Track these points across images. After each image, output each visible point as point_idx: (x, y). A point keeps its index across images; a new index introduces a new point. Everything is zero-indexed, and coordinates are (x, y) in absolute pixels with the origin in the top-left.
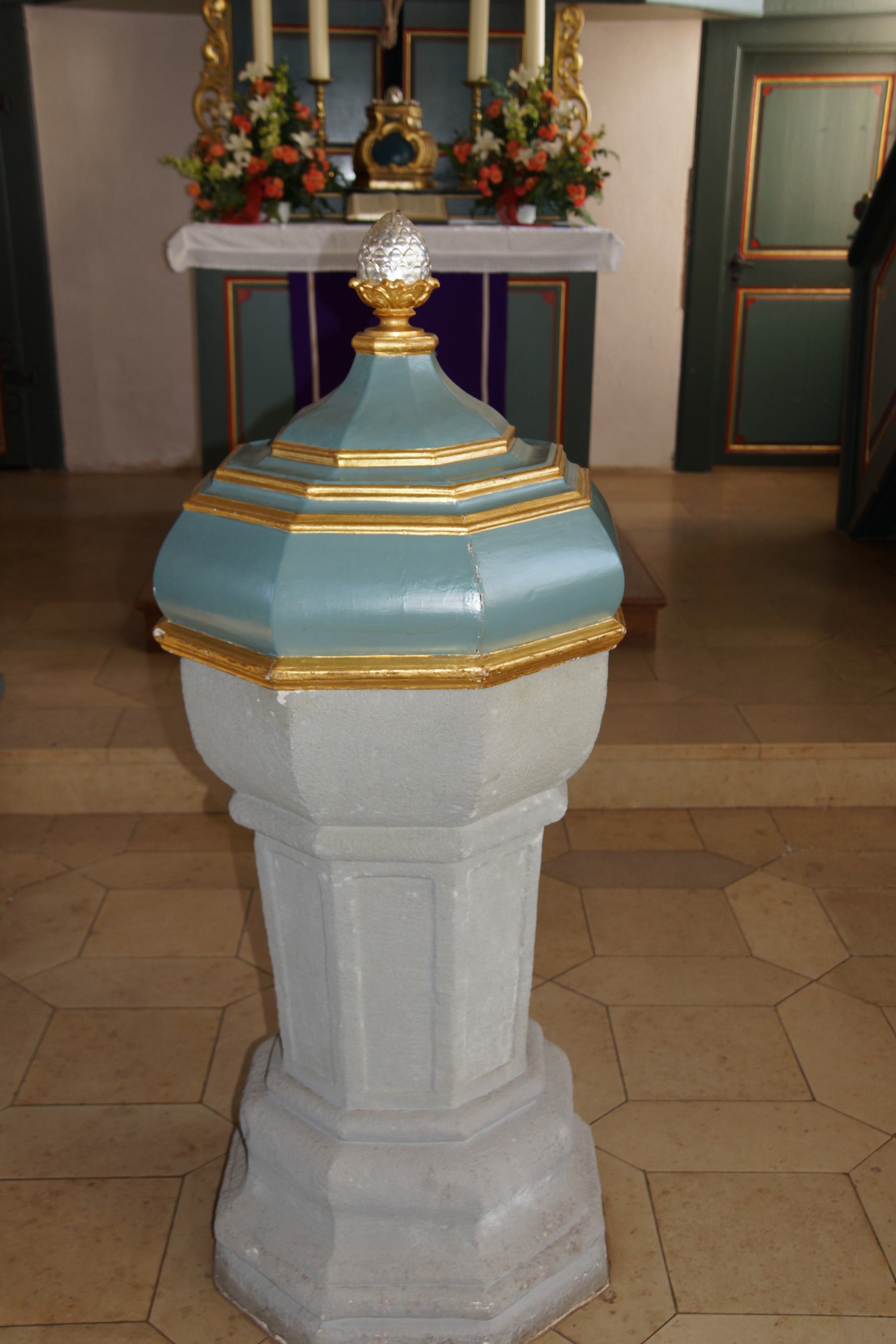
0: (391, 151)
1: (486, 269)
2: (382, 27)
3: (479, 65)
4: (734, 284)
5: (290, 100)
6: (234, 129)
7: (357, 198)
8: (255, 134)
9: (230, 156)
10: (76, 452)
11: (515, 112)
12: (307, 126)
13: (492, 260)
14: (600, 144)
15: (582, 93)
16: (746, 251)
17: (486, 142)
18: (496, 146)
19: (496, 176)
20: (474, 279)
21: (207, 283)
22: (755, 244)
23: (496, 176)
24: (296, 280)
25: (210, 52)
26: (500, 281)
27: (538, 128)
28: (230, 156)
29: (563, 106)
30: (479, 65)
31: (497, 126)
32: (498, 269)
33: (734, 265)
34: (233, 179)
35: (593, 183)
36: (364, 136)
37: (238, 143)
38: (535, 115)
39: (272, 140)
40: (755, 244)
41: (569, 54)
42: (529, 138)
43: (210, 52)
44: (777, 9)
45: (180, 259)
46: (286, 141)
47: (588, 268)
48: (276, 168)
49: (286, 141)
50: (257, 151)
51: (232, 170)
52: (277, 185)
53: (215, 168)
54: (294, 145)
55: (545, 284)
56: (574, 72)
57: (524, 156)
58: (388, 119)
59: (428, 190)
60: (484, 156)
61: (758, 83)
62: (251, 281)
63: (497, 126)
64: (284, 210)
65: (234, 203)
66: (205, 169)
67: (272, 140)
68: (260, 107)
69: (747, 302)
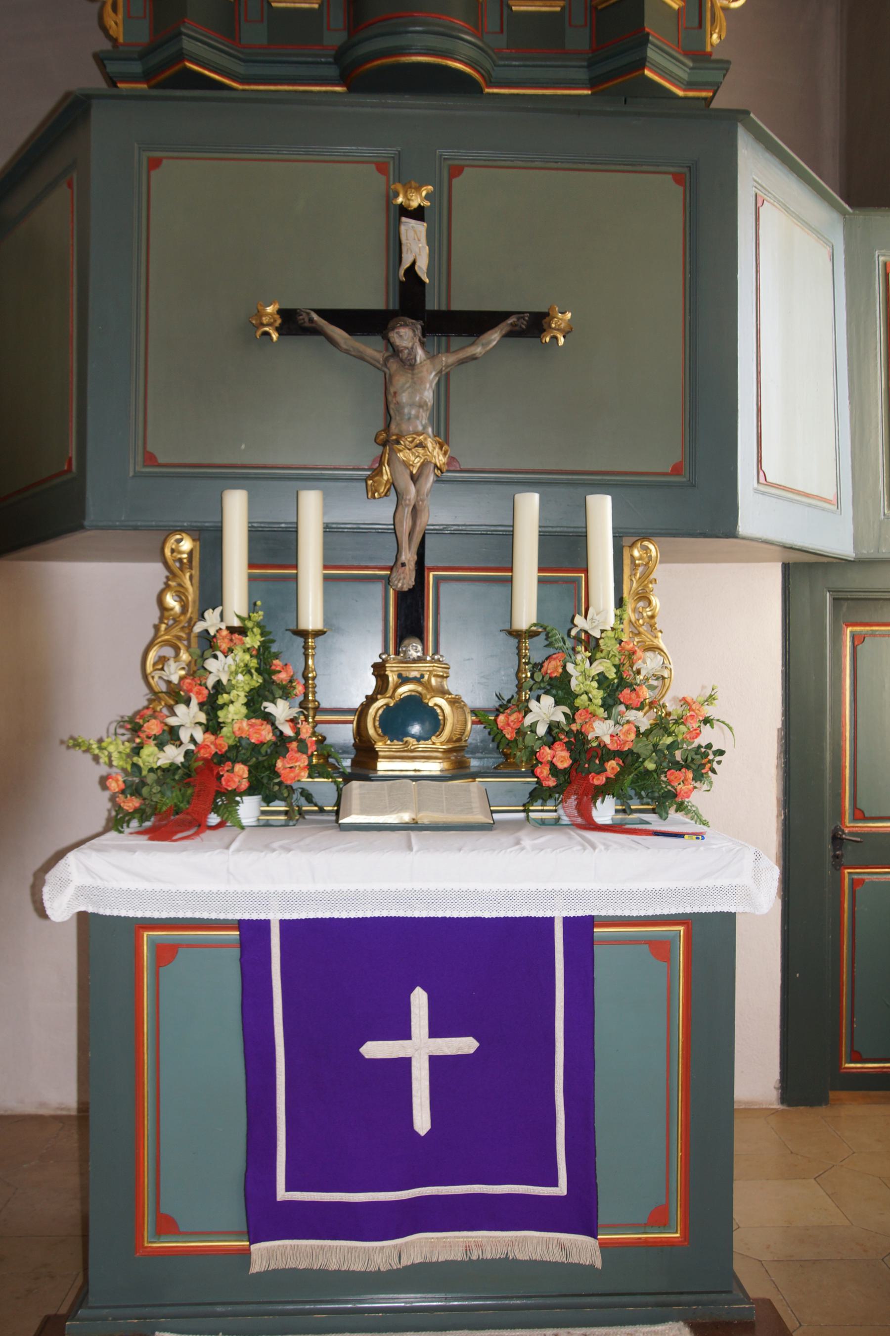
0: (407, 716)
1: (559, 912)
2: (397, 564)
4: (838, 863)
5: (264, 657)
11: (582, 673)
12: (286, 692)
13: (569, 896)
14: (708, 711)
15: (662, 645)
16: (850, 825)
17: (545, 711)
18: (559, 715)
19: (562, 758)
23: (562, 758)
24: (253, 932)
25: (171, 601)
26: (581, 929)
27: (615, 691)
28: (172, 735)
29: (649, 664)
33: (837, 839)
34: (172, 769)
36: (371, 699)
37: (188, 717)
38: (612, 674)
40: (859, 815)
41: (643, 597)
42: (607, 706)
43: (171, 601)
44: (868, 552)
45: (62, 902)
50: (213, 726)
54: (269, 718)
55: (654, 935)
57: (602, 730)
58: (404, 680)
59: (459, 769)
60: (541, 730)
62: (175, 937)
64: (249, 808)
66: (137, 750)
67: (234, 713)
69: (855, 883)
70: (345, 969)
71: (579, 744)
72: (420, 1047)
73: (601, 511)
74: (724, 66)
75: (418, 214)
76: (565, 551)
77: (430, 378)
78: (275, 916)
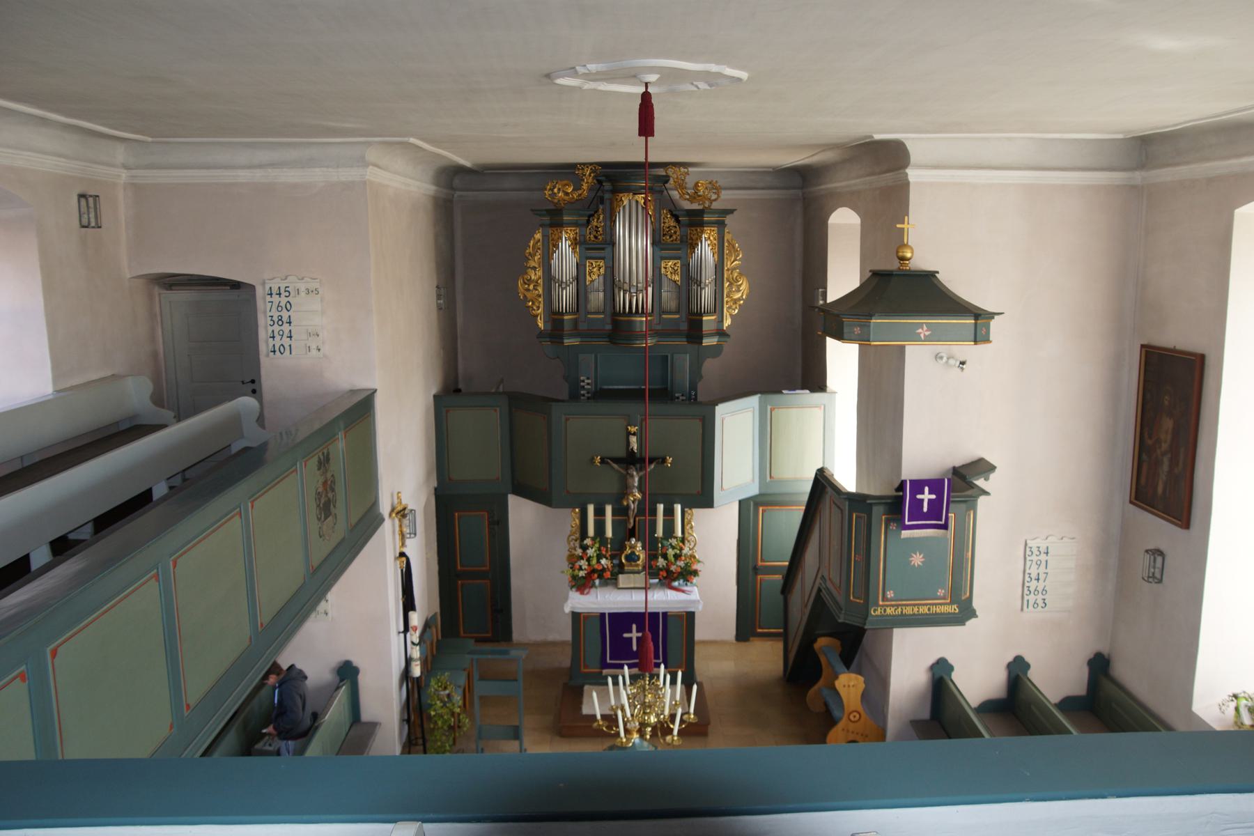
1: (661, 611)
3: (660, 532)
4: (756, 574)
6: (582, 558)
8: (589, 560)
9: (580, 568)
10: (516, 636)
11: (671, 552)
16: (760, 563)
21: (576, 616)
22: (762, 560)
24: (603, 615)
26: (665, 614)
28: (580, 568)
29: (686, 551)
30: (660, 532)
31: (665, 556)
35: (695, 573)
37: (583, 563)
39: (594, 561)
41: (690, 522)
45: (567, 609)
46: (598, 562)
48: (594, 571)
49: (598, 562)
51: (582, 573)
63: (665, 556)
65: (582, 584)
67: (594, 561)
68: (591, 552)
70: (622, 620)
71: (667, 570)
72: (634, 635)
73: (678, 508)
74: (728, 336)
75: (634, 434)
76: (669, 512)
77: (637, 479)
78: (607, 612)
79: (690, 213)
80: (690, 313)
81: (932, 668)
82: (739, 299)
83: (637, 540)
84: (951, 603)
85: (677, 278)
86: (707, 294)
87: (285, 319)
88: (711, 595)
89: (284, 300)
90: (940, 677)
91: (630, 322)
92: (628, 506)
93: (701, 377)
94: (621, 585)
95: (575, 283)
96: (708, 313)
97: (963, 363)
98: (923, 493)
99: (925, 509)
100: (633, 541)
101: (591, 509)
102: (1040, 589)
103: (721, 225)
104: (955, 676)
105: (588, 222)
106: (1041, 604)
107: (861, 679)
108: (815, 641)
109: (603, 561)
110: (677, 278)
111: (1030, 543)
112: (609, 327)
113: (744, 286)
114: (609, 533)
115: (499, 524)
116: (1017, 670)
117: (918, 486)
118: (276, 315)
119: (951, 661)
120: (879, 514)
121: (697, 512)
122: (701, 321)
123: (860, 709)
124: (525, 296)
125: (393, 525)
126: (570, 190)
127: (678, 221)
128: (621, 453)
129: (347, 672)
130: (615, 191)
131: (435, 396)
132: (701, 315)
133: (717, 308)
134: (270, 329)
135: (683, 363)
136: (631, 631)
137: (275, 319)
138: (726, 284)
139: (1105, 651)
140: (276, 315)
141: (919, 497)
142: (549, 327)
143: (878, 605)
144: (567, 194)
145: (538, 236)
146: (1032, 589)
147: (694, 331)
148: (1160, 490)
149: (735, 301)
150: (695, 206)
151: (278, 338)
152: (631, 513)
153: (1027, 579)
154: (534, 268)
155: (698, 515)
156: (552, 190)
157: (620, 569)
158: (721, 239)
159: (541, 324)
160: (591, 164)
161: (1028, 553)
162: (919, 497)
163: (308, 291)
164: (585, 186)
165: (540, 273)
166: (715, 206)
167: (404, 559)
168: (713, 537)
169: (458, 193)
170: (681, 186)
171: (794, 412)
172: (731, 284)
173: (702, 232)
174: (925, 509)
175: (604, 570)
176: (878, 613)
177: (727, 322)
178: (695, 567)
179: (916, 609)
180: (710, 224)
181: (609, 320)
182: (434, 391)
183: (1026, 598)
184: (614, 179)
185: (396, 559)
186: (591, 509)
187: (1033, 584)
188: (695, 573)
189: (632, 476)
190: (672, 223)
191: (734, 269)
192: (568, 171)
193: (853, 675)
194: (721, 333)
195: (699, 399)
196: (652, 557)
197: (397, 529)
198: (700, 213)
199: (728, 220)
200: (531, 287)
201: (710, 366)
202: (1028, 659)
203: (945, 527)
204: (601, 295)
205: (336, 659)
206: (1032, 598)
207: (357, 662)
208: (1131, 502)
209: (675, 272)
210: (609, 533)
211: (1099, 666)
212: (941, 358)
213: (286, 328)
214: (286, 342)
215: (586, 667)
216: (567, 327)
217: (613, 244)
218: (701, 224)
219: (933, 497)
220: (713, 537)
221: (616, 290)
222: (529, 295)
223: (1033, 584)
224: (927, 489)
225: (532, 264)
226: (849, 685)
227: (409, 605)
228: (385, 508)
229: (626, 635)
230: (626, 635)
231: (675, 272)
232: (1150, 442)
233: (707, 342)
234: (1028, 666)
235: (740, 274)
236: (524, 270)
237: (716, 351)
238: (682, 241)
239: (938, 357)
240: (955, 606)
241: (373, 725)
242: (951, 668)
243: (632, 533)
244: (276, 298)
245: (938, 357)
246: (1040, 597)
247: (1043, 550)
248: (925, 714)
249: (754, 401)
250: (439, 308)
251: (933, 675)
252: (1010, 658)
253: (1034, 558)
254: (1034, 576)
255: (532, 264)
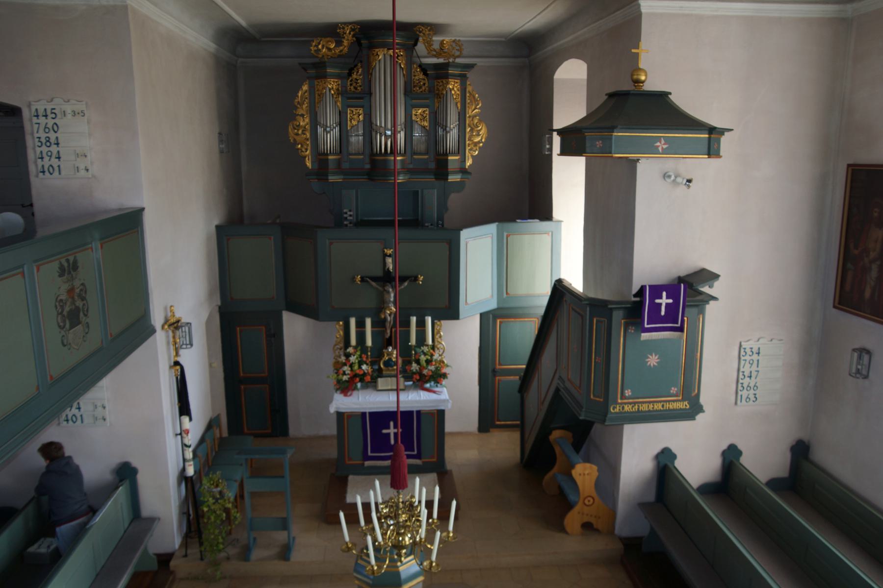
1: (415, 409)
3: (413, 341)
4: (495, 376)
6: (345, 364)
7: (380, 380)
8: (351, 366)
9: (344, 373)
10: (292, 431)
11: (423, 358)
16: (498, 367)
20: (411, 413)
21: (340, 415)
23: (418, 378)
24: (364, 414)
26: (419, 412)
28: (344, 373)
29: (436, 356)
30: (413, 341)
32: (418, 409)
35: (444, 376)
37: (346, 369)
39: (356, 367)
40: (500, 364)
41: (439, 332)
44: (501, 306)
45: (332, 410)
46: (360, 367)
47: (442, 408)
48: (356, 376)
49: (360, 367)
50: (352, 370)
51: (345, 378)
52: (358, 379)
53: (340, 376)
56: (440, 337)
61: (498, 321)
62: (351, 415)
63: (418, 362)
65: (346, 388)
67: (356, 367)
68: (353, 359)
70: (380, 418)
71: (420, 373)
72: (392, 431)
73: (429, 320)
74: (470, 173)
75: (390, 256)
76: (421, 324)
77: (392, 295)
78: (368, 411)
79: (436, 66)
80: (437, 154)
81: (657, 457)
82: (479, 142)
83: (395, 348)
84: (683, 400)
85: (426, 124)
86: (453, 136)
87: (53, 140)
88: (457, 393)
89: (50, 122)
90: (664, 465)
91: (386, 161)
92: (385, 319)
93: (447, 209)
94: (380, 388)
95: (337, 129)
96: (453, 154)
97: (689, 181)
98: (661, 298)
99: (663, 313)
100: (390, 349)
101: (353, 322)
102: (752, 385)
103: (463, 78)
104: (679, 464)
105: (350, 74)
106: (752, 398)
107: (595, 468)
108: (550, 433)
109: (364, 367)
110: (426, 124)
111: (744, 345)
112: (368, 166)
113: (483, 131)
114: (369, 343)
115: (276, 336)
116: (731, 457)
117: (656, 291)
118: (43, 136)
119: (674, 450)
120: (618, 317)
121: (444, 323)
122: (447, 160)
123: (594, 494)
124: (295, 140)
125: (168, 337)
126: (332, 46)
127: (425, 74)
128: (379, 273)
129: (126, 473)
130: (372, 47)
131: (217, 227)
132: (446, 155)
133: (461, 150)
134: (38, 150)
135: (431, 197)
136: (388, 428)
137: (43, 140)
138: (468, 130)
139: (805, 438)
140: (43, 136)
141: (658, 301)
142: (316, 167)
143: (617, 403)
144: (329, 49)
145: (305, 87)
146: (745, 385)
147: (441, 169)
148: (867, 294)
149: (476, 144)
150: (441, 60)
151: (46, 159)
152: (388, 325)
153: (741, 376)
154: (303, 115)
155: (446, 326)
156: (317, 46)
157: (379, 373)
158: (463, 90)
159: (309, 164)
160: (350, 23)
161: (742, 353)
162: (658, 301)
163: (74, 114)
164: (346, 43)
165: (307, 120)
166: (458, 60)
167: (178, 367)
168: (459, 345)
169: (240, 60)
170: (429, 44)
171: (527, 238)
172: (472, 130)
173: (448, 83)
174: (663, 313)
175: (365, 374)
176: (617, 410)
177: (469, 162)
178: (444, 370)
179: (651, 406)
180: (455, 76)
181: (367, 160)
182: (216, 222)
183: (740, 393)
184: (370, 35)
185: (171, 367)
186: (353, 322)
187: (746, 381)
188: (444, 376)
189: (388, 292)
190: (422, 76)
191: (475, 116)
192: (331, 31)
193: (588, 465)
194: (463, 171)
195: (445, 226)
196: (407, 363)
197: (171, 340)
198: (445, 66)
199: (470, 75)
200: (300, 132)
201: (454, 199)
202: (740, 447)
203: (681, 329)
204: (361, 138)
205: (115, 460)
206: (745, 393)
207: (135, 463)
208: (834, 307)
209: (423, 119)
210: (369, 343)
211: (801, 451)
212: (669, 177)
213: (54, 149)
214: (55, 162)
215: (350, 459)
216: (331, 166)
217: (371, 94)
218: (446, 76)
219: (670, 301)
220: (459, 345)
221: (374, 134)
222: (298, 139)
223: (746, 381)
224: (664, 294)
225: (300, 112)
226: (585, 474)
227: (184, 409)
228: (157, 318)
229: (385, 431)
230: (385, 431)
231: (423, 119)
232: (856, 252)
233: (452, 178)
234: (740, 453)
235: (480, 121)
236: (294, 117)
237: (460, 186)
238: (430, 91)
239: (666, 176)
240: (686, 403)
241: (152, 520)
242: (674, 457)
243: (389, 342)
244: (42, 120)
245: (666, 176)
246: (752, 392)
247: (755, 350)
248: (651, 497)
249: (492, 228)
250: (221, 152)
251: (658, 463)
252: (724, 446)
253: (747, 358)
254: (747, 374)
255: (300, 112)
